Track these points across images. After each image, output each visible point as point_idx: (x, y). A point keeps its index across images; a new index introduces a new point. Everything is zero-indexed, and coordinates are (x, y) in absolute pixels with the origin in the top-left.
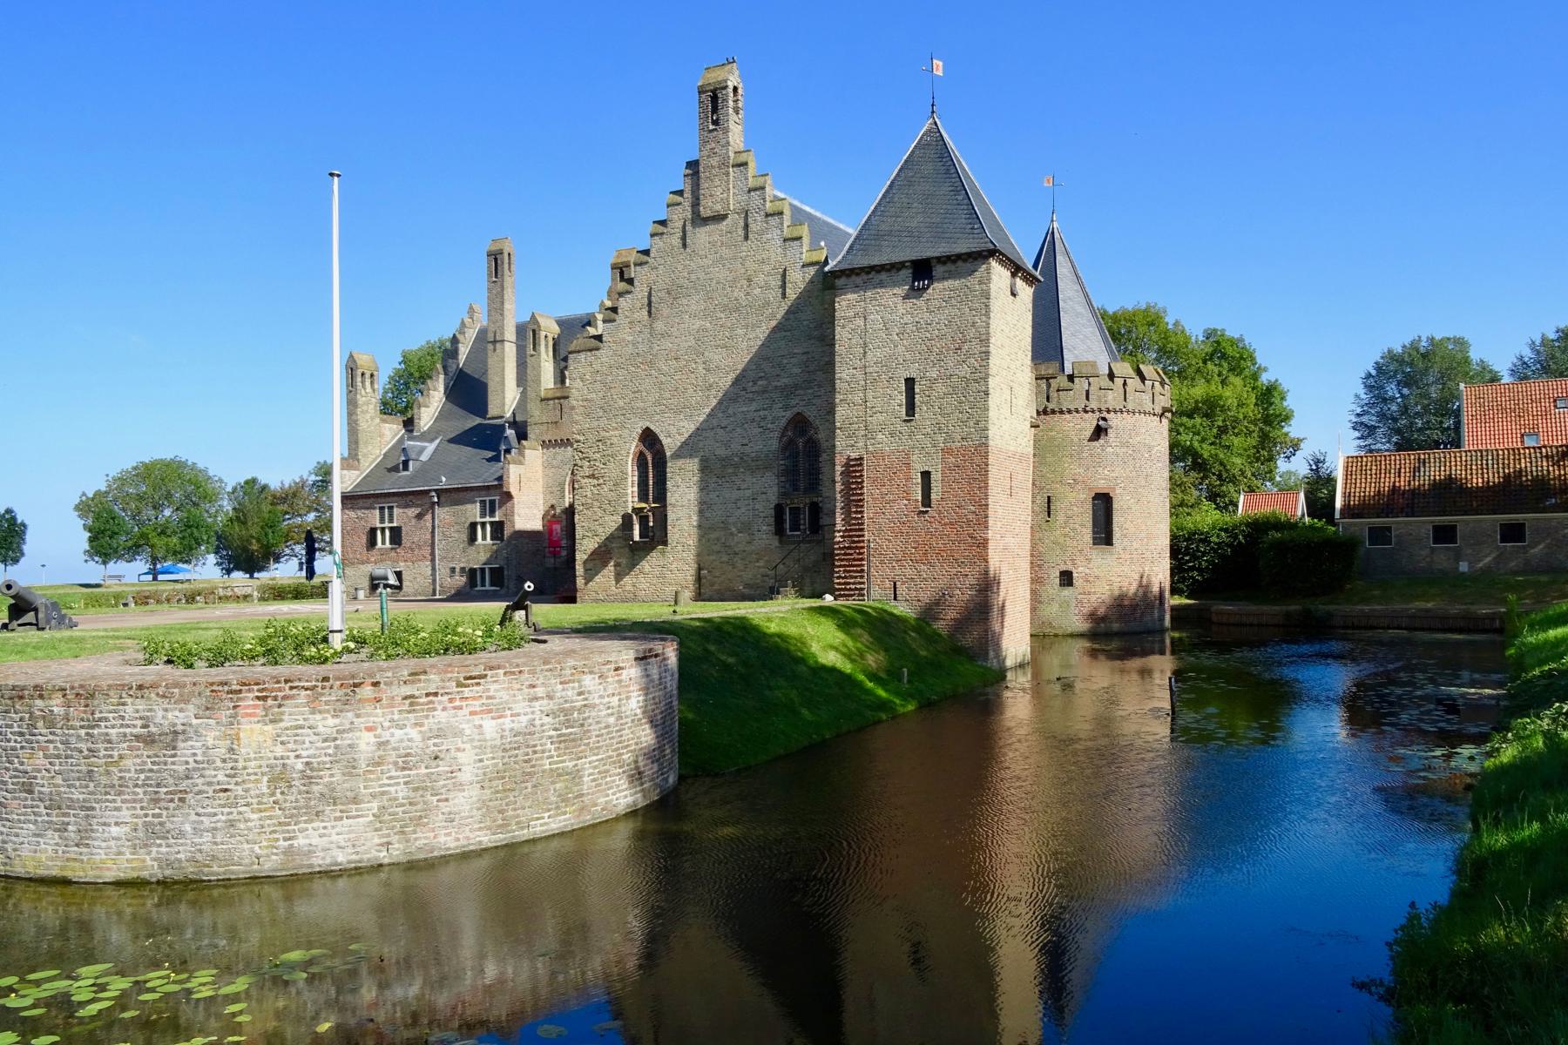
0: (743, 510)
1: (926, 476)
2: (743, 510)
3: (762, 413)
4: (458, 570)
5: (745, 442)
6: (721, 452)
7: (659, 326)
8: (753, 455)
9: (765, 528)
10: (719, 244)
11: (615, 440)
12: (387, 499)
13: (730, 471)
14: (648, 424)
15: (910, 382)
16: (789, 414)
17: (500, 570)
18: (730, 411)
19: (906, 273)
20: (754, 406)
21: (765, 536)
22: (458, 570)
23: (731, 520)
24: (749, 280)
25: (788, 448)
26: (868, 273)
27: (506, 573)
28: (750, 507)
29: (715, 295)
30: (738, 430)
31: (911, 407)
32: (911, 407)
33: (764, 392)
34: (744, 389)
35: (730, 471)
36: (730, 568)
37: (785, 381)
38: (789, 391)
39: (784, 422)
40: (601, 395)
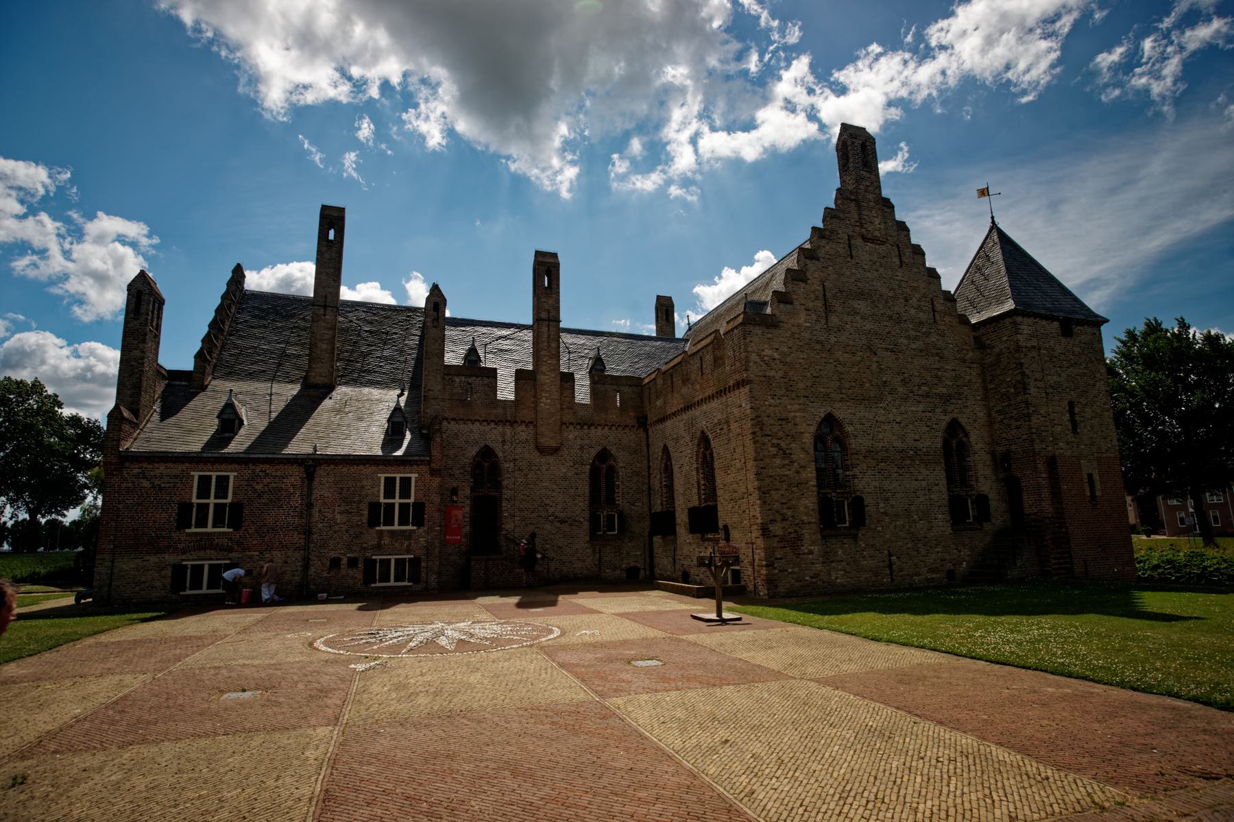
0: (922, 499)
1: (1090, 476)
2: (922, 499)
3: (928, 414)
4: (345, 561)
5: (917, 438)
6: (898, 444)
7: (834, 320)
8: (924, 450)
9: (940, 516)
10: (878, 264)
11: (798, 420)
12: (217, 466)
13: (908, 462)
14: (829, 409)
15: (1071, 404)
16: (947, 418)
17: (415, 562)
18: (903, 409)
19: (1056, 324)
20: (921, 407)
21: (941, 523)
22: (345, 561)
23: (913, 508)
24: (906, 300)
25: (946, 444)
26: (1035, 318)
27: (423, 564)
28: (927, 497)
29: (881, 306)
30: (911, 426)
31: (1075, 425)
32: (1075, 425)
33: (928, 396)
34: (912, 392)
35: (908, 462)
36: (916, 553)
37: (942, 390)
38: (946, 399)
39: (943, 425)
40: (780, 374)
